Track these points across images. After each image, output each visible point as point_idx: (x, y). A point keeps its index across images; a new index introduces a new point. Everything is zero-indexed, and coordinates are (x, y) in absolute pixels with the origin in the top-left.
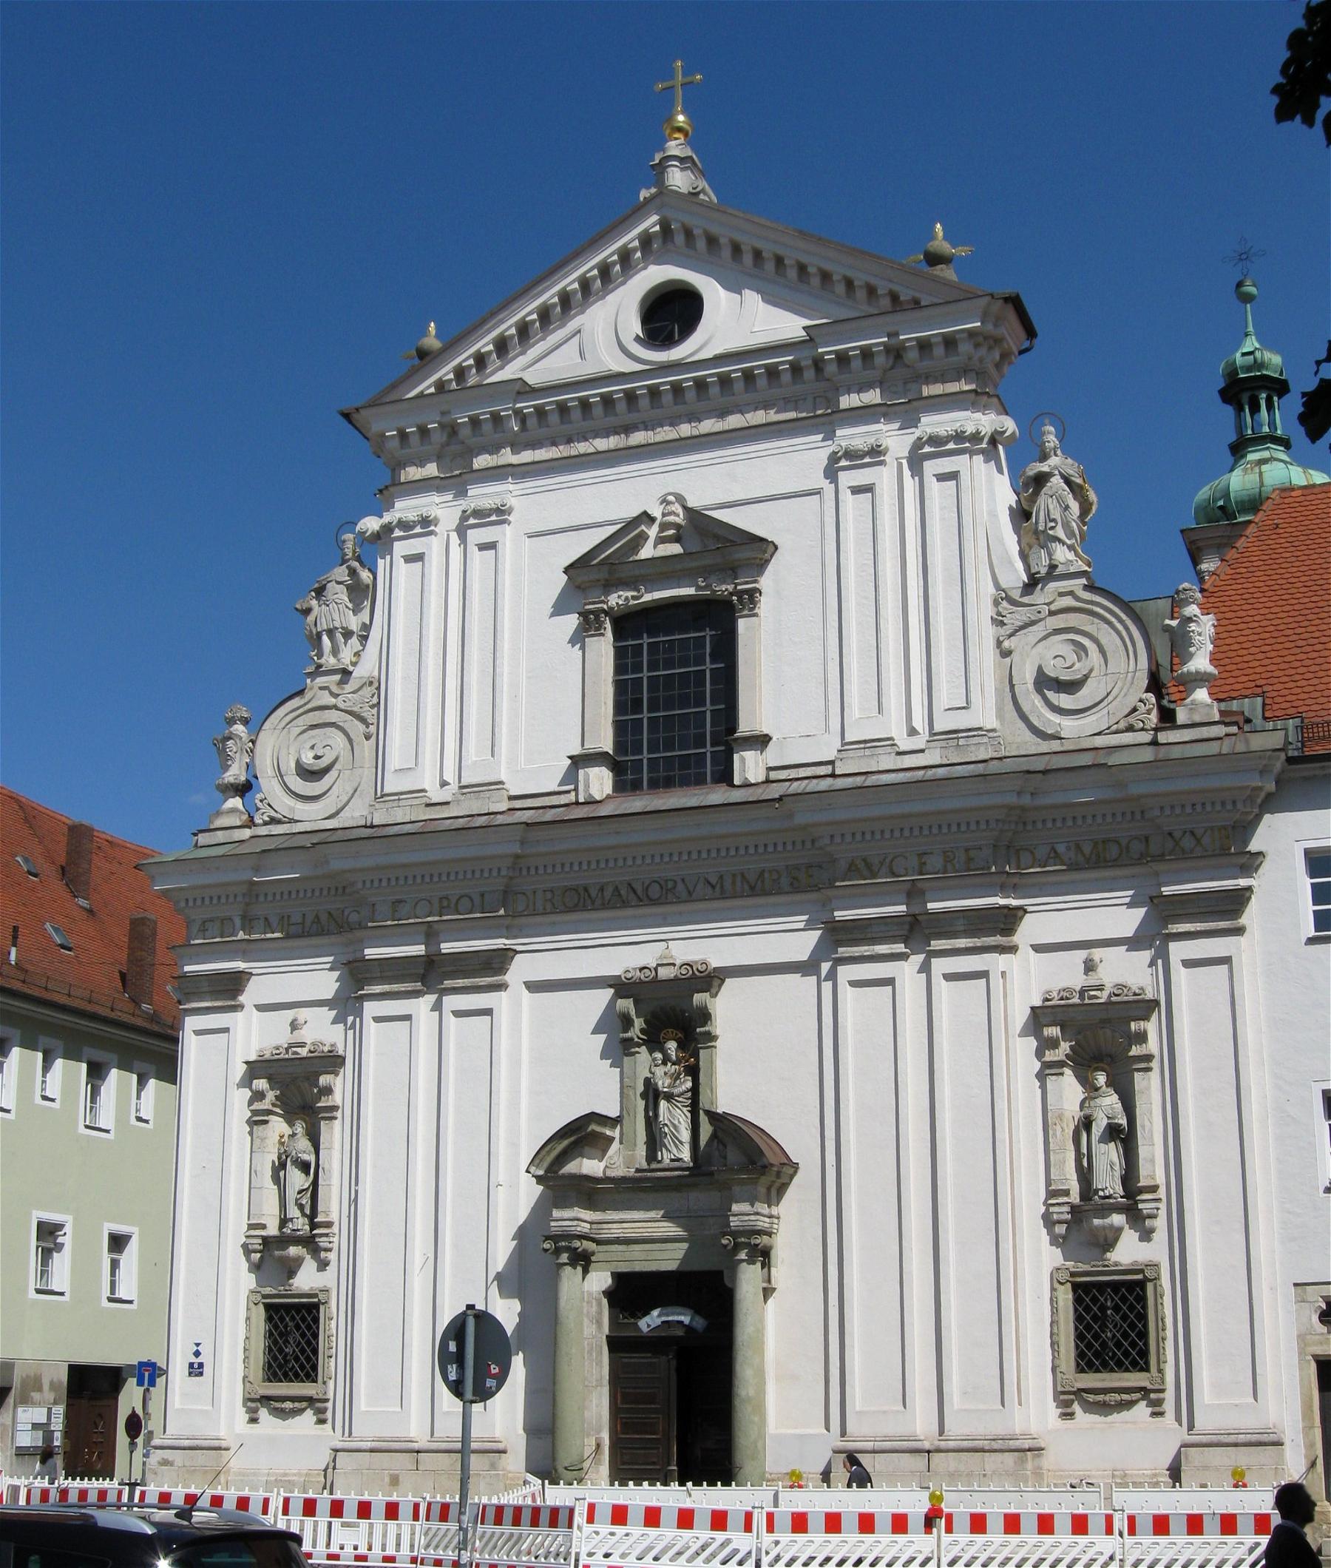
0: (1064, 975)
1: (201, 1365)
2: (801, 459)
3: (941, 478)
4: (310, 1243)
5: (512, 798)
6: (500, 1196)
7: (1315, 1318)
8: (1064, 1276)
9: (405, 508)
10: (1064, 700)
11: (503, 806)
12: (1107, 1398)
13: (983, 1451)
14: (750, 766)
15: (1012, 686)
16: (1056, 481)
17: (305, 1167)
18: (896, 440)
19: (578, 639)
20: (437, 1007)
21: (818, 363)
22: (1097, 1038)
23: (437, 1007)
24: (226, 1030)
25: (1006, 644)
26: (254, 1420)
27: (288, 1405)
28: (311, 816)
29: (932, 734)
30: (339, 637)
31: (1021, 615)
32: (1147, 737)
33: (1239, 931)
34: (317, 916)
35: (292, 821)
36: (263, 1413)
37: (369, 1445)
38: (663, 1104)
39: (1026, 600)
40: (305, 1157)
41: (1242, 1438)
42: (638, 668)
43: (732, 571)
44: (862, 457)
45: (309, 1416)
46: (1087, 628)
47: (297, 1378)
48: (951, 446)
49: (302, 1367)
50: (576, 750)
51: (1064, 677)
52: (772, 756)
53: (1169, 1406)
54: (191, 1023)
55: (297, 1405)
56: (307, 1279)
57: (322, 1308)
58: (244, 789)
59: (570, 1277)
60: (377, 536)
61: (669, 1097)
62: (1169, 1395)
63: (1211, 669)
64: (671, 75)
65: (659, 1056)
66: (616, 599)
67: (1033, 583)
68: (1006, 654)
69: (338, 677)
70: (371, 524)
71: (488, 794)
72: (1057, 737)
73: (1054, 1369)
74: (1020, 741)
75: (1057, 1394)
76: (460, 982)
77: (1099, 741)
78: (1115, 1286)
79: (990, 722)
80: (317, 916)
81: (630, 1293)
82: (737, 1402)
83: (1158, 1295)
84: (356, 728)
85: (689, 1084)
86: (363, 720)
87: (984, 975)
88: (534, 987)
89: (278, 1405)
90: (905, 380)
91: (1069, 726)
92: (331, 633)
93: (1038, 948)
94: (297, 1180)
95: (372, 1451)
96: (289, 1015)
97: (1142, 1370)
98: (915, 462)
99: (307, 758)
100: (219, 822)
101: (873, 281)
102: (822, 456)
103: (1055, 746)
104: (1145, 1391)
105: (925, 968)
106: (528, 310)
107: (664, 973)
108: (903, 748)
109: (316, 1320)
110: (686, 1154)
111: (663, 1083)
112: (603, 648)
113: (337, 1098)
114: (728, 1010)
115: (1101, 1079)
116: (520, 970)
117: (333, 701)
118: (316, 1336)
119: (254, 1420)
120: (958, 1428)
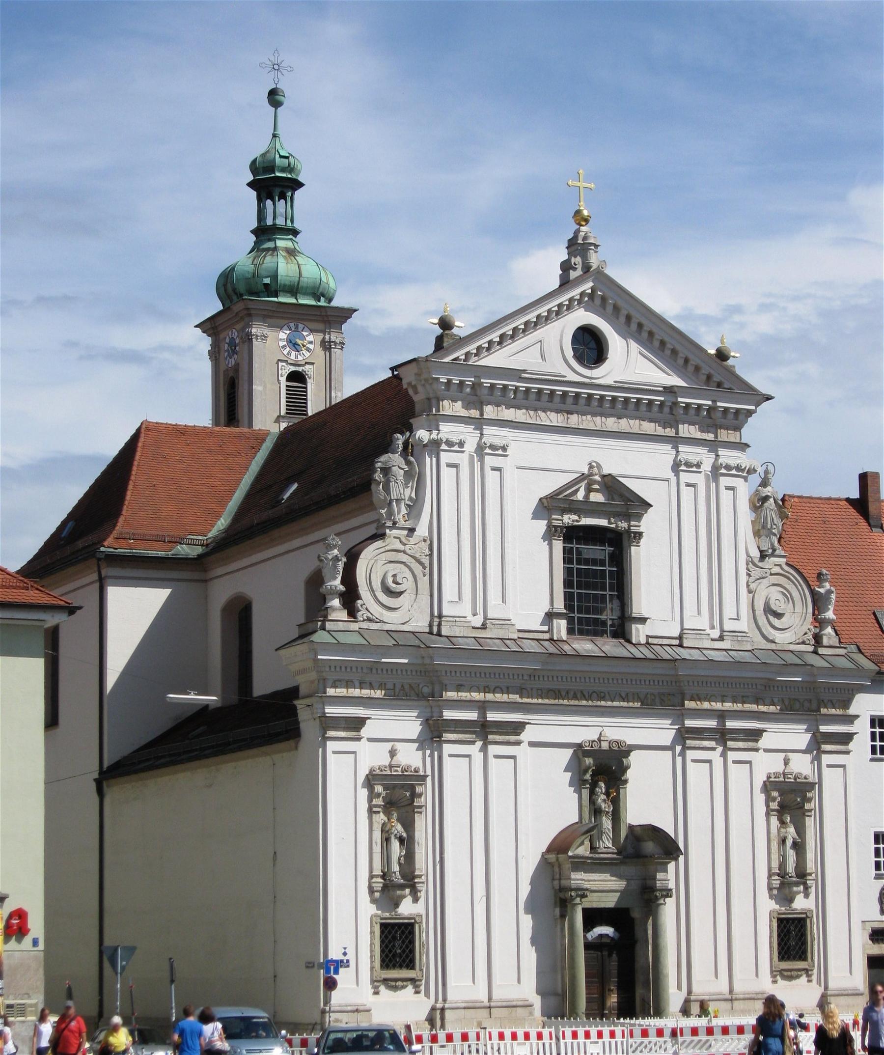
1: (348, 961)
2: (658, 458)
5: (519, 631)
8: (776, 915)
9: (447, 430)
14: (639, 633)
16: (772, 500)
18: (707, 460)
22: (791, 800)
26: (376, 993)
27: (400, 983)
32: (811, 649)
33: (848, 753)
34: (402, 686)
36: (382, 988)
37: (463, 1005)
39: (760, 564)
41: (850, 992)
43: (628, 517)
44: (692, 467)
48: (734, 472)
53: (814, 977)
54: (331, 746)
62: (815, 971)
63: (835, 617)
66: (569, 519)
67: (763, 556)
69: (406, 532)
71: (507, 627)
72: (773, 642)
75: (772, 971)
80: (402, 686)
95: (465, 1008)
96: (389, 745)
105: (724, 755)
107: (605, 746)
112: (558, 546)
116: (528, 735)
117: (402, 547)
119: (376, 993)
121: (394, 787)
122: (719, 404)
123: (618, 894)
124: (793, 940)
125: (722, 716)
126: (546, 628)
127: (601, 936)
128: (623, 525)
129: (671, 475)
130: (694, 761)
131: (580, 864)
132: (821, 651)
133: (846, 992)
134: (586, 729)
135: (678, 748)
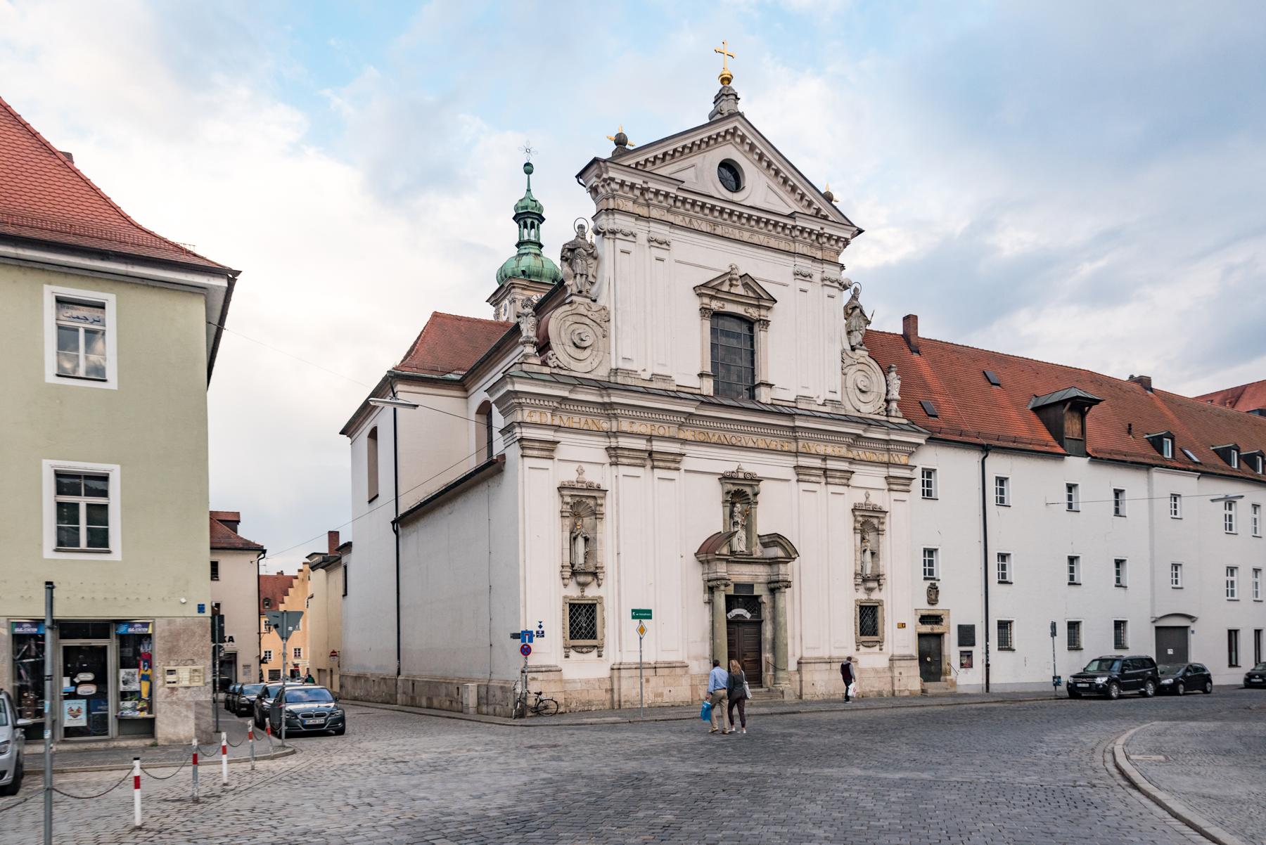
11: (675, 389)
22: (868, 522)
36: (572, 653)
47: (586, 637)
57: (598, 606)
66: (715, 305)
112: (708, 324)
119: (567, 657)
128: (753, 313)
134: (729, 462)
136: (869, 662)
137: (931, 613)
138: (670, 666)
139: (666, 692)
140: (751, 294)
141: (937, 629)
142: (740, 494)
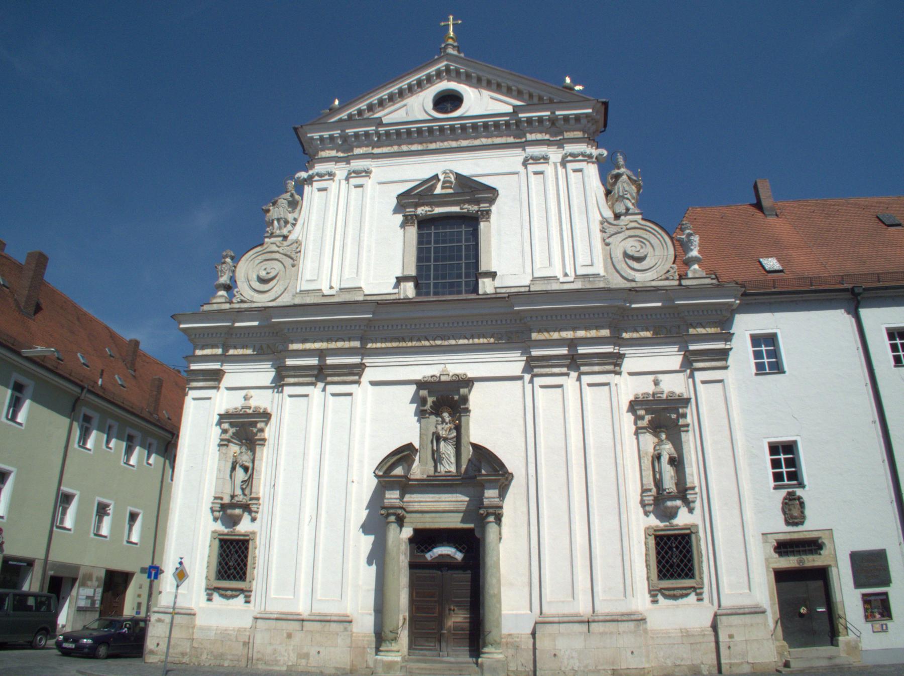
0: (645, 386)
3: (575, 171)
4: (246, 508)
5: (365, 295)
6: (354, 488)
7: (772, 550)
8: (652, 532)
9: (319, 168)
10: (635, 265)
12: (675, 592)
13: (618, 621)
14: (486, 286)
15: (611, 258)
17: (246, 469)
18: (555, 155)
19: (403, 225)
20: (324, 390)
21: (519, 122)
22: (662, 417)
23: (324, 390)
24: (209, 398)
25: (607, 241)
26: (210, 600)
27: (229, 593)
28: (262, 300)
29: (576, 275)
30: (282, 222)
31: (612, 230)
32: (676, 283)
33: (726, 368)
35: (252, 302)
36: (216, 596)
37: (275, 616)
38: (442, 444)
39: (615, 222)
40: (247, 464)
41: (747, 610)
42: (429, 242)
43: (477, 202)
45: (241, 598)
46: (644, 236)
47: (235, 578)
48: (580, 158)
49: (238, 573)
50: (399, 274)
51: (636, 255)
52: (498, 282)
53: (706, 596)
55: (234, 593)
56: (244, 526)
57: (251, 542)
58: (228, 288)
59: (393, 528)
60: (305, 180)
61: (445, 439)
62: (706, 590)
63: (699, 256)
64: (448, 20)
65: (440, 419)
66: (421, 211)
67: (617, 216)
68: (608, 244)
69: (281, 239)
70: (303, 175)
72: (633, 281)
73: (648, 578)
74: (617, 282)
75: (650, 591)
76: (336, 379)
77: (654, 284)
78: (676, 536)
79: (602, 273)
81: (424, 539)
82: (487, 597)
83: (698, 540)
84: (288, 262)
85: (455, 434)
86: (292, 258)
87: (608, 384)
88: (374, 383)
89: (223, 592)
90: (556, 130)
91: (638, 276)
92: (278, 220)
93: (631, 374)
94: (240, 474)
96: (244, 392)
97: (691, 578)
98: (564, 163)
99: (263, 274)
100: (215, 301)
101: (542, 93)
102: (521, 159)
103: (633, 285)
104: (694, 589)
106: (384, 94)
107: (443, 378)
108: (561, 280)
109: (247, 548)
110: (453, 469)
111: (443, 433)
112: (413, 231)
113: (266, 434)
114: (477, 397)
115: (663, 436)
116: (369, 374)
118: (246, 557)
119: (210, 600)
120: (603, 608)
121: (243, 424)
122: (557, 113)
123: (461, 515)
124: (675, 558)
125: (572, 344)
126: (396, 291)
127: (441, 556)
129: (521, 169)
130: (542, 387)
131: (406, 486)
132: (684, 282)
133: (742, 611)
135: (527, 377)
136: (686, 615)
137: (795, 536)
138: (325, 620)
139: (313, 651)
140: (467, 190)
141: (812, 561)
142: (444, 401)
